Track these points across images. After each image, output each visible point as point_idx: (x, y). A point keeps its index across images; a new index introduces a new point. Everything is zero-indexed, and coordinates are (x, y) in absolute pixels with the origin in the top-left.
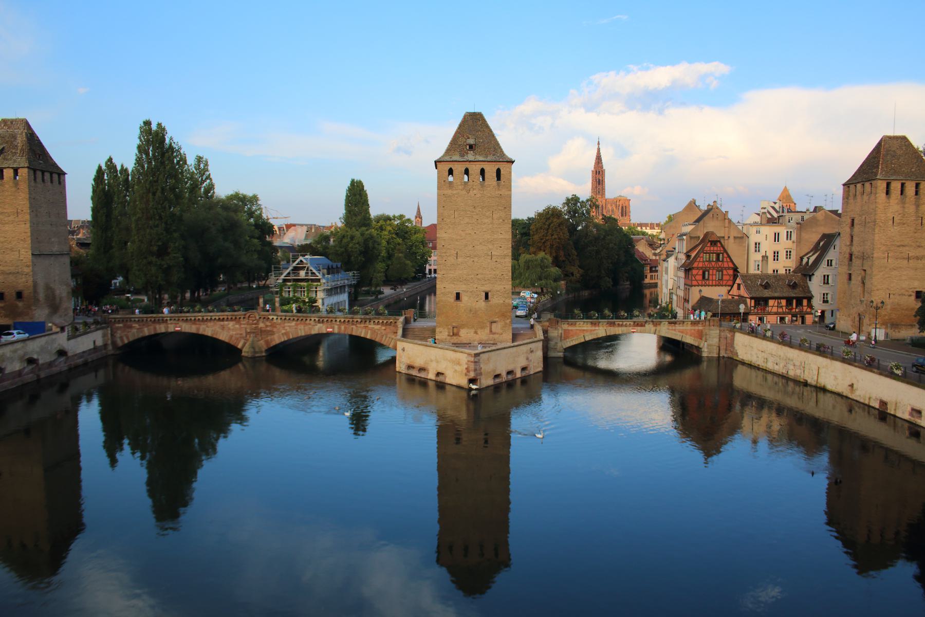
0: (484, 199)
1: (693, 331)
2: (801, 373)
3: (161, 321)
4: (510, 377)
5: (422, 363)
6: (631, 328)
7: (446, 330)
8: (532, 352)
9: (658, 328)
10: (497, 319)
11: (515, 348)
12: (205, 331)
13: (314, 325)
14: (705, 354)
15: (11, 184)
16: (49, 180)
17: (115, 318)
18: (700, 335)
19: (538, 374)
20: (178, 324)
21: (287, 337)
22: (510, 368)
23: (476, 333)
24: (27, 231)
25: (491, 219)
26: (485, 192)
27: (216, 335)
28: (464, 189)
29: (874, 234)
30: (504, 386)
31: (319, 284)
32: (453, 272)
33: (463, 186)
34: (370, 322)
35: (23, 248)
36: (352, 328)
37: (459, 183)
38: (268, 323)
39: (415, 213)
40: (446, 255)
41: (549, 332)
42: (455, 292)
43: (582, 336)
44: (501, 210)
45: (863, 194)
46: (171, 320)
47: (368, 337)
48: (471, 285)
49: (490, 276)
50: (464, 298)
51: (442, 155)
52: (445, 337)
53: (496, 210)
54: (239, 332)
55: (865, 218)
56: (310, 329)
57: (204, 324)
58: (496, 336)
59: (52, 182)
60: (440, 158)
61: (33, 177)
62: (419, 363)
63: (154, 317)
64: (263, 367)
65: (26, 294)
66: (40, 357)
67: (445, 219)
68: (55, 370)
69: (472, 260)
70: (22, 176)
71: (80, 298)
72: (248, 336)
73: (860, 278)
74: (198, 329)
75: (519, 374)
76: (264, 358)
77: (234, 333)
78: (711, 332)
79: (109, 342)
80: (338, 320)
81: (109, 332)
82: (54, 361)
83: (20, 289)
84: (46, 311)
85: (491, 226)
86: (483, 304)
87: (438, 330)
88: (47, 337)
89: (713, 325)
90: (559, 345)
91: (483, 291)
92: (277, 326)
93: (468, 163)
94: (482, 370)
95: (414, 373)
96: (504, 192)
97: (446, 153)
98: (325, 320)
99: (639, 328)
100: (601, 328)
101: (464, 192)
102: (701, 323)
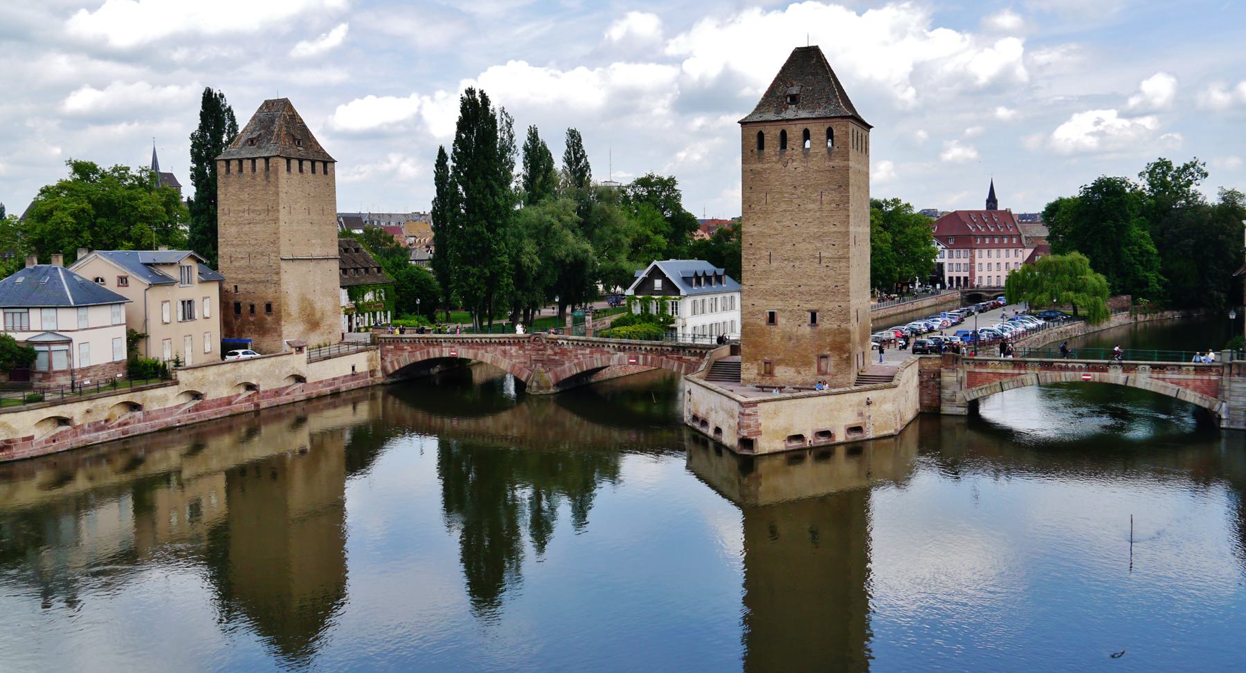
0: (809, 175)
1: (1198, 383)
3: (435, 343)
4: (823, 441)
6: (1082, 373)
7: (755, 366)
8: (868, 404)
9: (1132, 375)
10: (829, 353)
11: (833, 398)
12: (483, 356)
13: (613, 354)
14: (1224, 425)
15: (262, 176)
16: (310, 170)
17: (385, 338)
18: (1216, 391)
19: (885, 441)
20: (454, 347)
21: (580, 369)
22: (822, 428)
23: (799, 373)
25: (818, 203)
26: (810, 165)
27: (497, 363)
28: (779, 160)
30: (809, 458)
31: (677, 297)
32: (763, 282)
33: (778, 158)
34: (684, 351)
35: (274, 252)
36: (662, 360)
37: (773, 153)
38: (557, 350)
39: (987, 196)
40: (755, 258)
41: (942, 374)
42: (768, 311)
43: (998, 383)
44: (834, 190)
46: (445, 341)
48: (790, 302)
49: (818, 288)
50: (781, 320)
51: (750, 113)
52: (753, 377)
53: (826, 190)
54: (522, 360)
56: (609, 359)
57: (482, 349)
58: (827, 378)
59: (313, 171)
60: (746, 118)
61: (286, 166)
62: (701, 413)
63: (427, 338)
64: (551, 409)
65: (274, 307)
66: (261, 383)
67: (753, 205)
68: (284, 399)
69: (792, 264)
70: (272, 166)
71: (389, 313)
72: (534, 365)
74: (476, 355)
75: (840, 436)
76: (552, 397)
77: (518, 361)
78: (1234, 385)
79: (379, 368)
80: (643, 348)
81: (379, 355)
82: (287, 387)
83: (270, 300)
84: (301, 327)
85: (818, 214)
86: (808, 329)
87: (743, 366)
88: (272, 359)
89: (1239, 374)
90: (959, 395)
91: (808, 311)
92: (569, 354)
93: (784, 123)
94: (761, 428)
95: (697, 425)
97: (756, 109)
98: (627, 347)
99: (1097, 374)
100: (1028, 372)
101: (779, 166)
102: (1214, 369)
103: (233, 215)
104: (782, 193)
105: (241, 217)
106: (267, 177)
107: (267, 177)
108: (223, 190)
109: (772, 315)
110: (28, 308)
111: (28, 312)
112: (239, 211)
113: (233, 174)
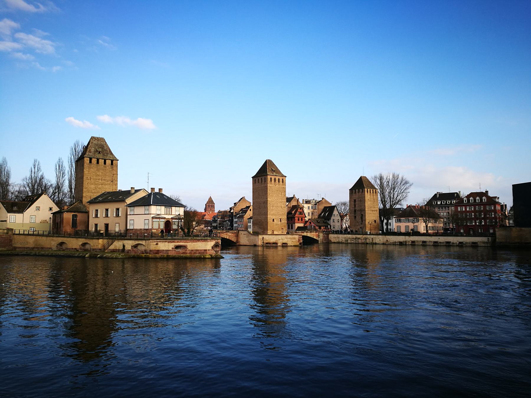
2: (364, 242)
5: (274, 241)
14: (319, 242)
15: (109, 167)
18: (319, 236)
23: (278, 233)
24: (116, 189)
29: (365, 204)
32: (272, 212)
45: (359, 192)
47: (228, 238)
50: (275, 221)
55: (361, 199)
73: (360, 217)
86: (280, 222)
96: (284, 186)
101: (274, 186)
103: (93, 180)
104: (275, 192)
105: (97, 182)
106: (112, 168)
107: (112, 168)
108: (87, 170)
109: (273, 219)
110: (172, 206)
111: (172, 208)
112: (97, 179)
113: (93, 164)
